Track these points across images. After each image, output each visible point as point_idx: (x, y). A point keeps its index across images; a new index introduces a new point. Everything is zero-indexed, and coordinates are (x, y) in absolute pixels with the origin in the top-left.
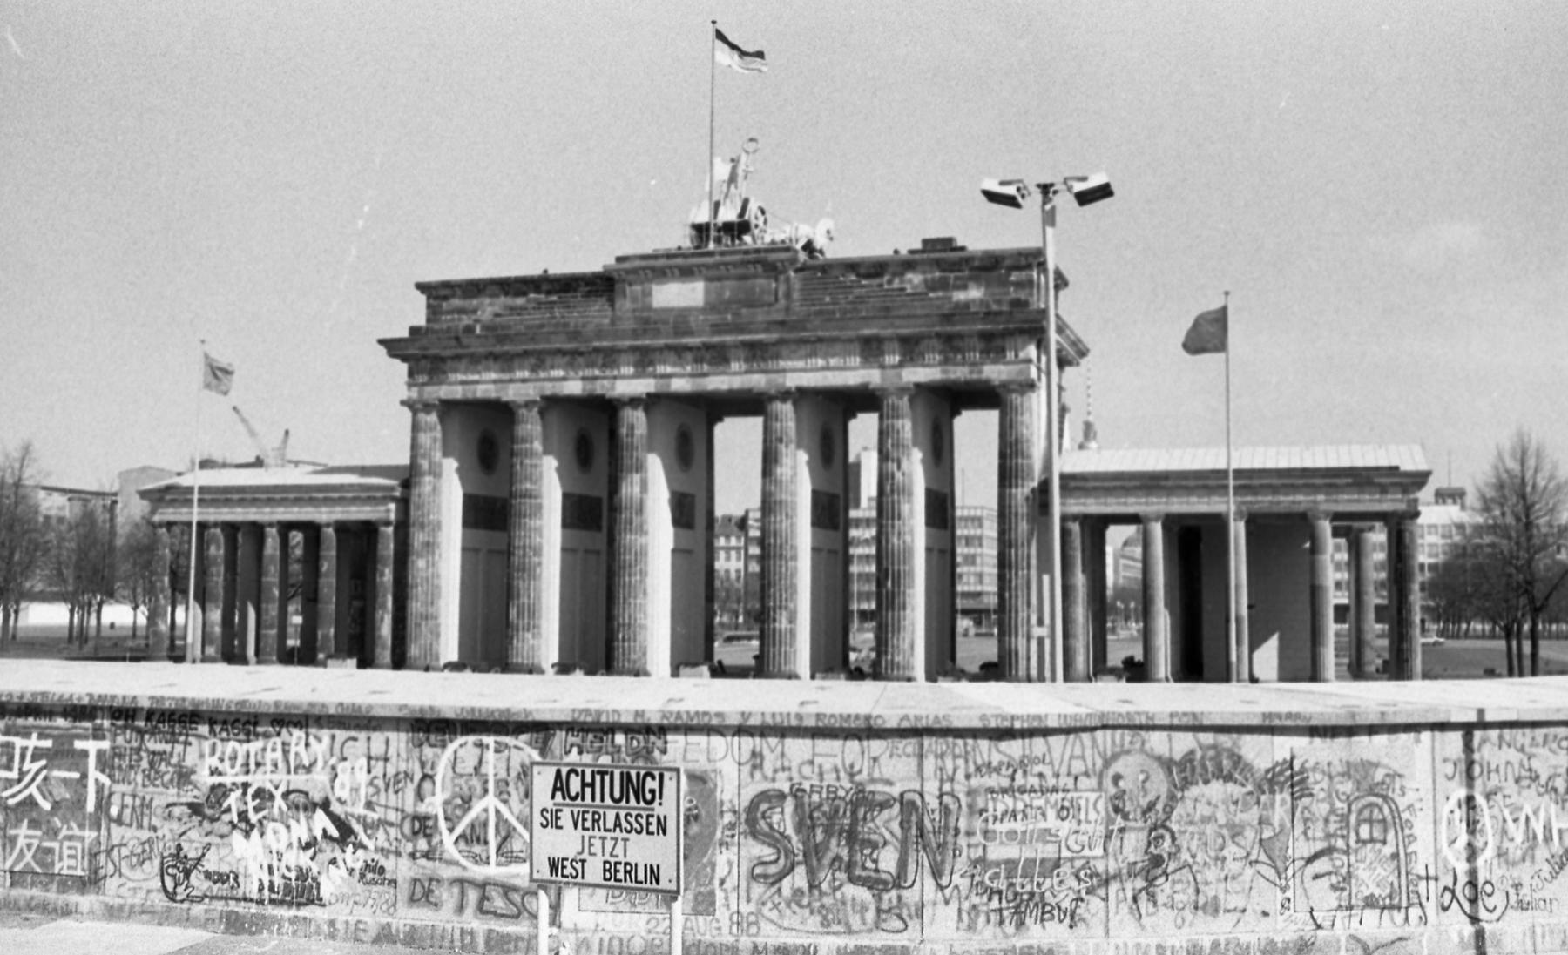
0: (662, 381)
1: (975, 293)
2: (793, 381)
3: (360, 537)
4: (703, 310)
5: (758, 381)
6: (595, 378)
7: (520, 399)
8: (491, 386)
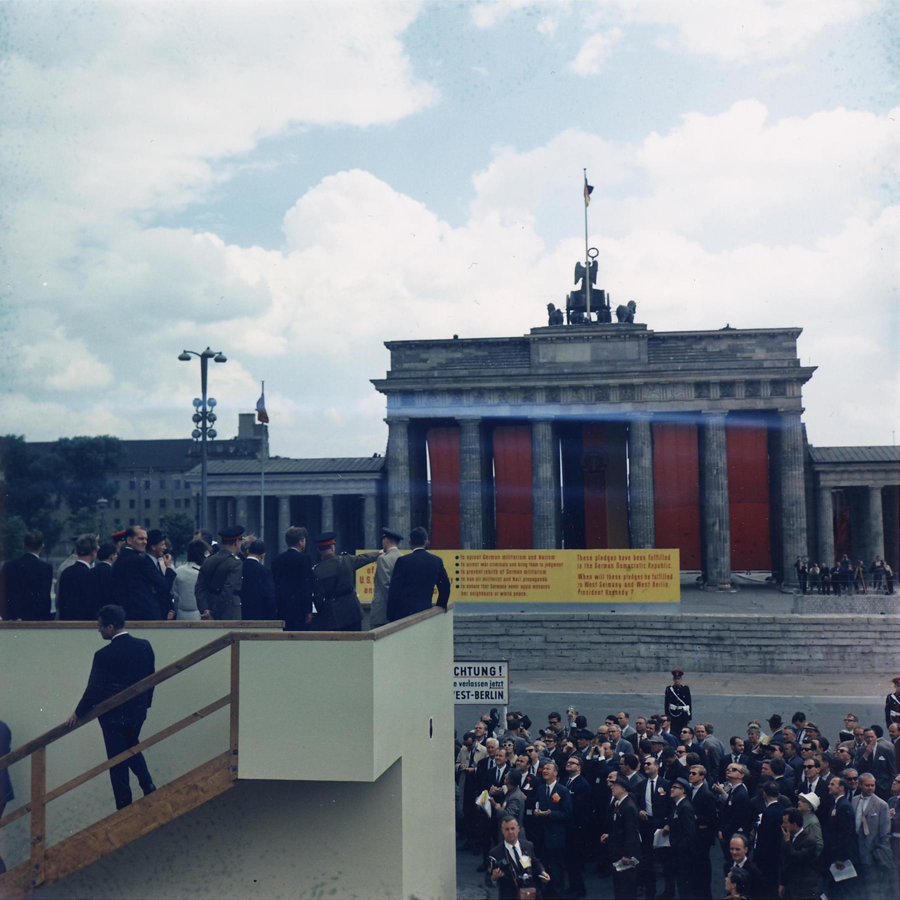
3: (349, 506)
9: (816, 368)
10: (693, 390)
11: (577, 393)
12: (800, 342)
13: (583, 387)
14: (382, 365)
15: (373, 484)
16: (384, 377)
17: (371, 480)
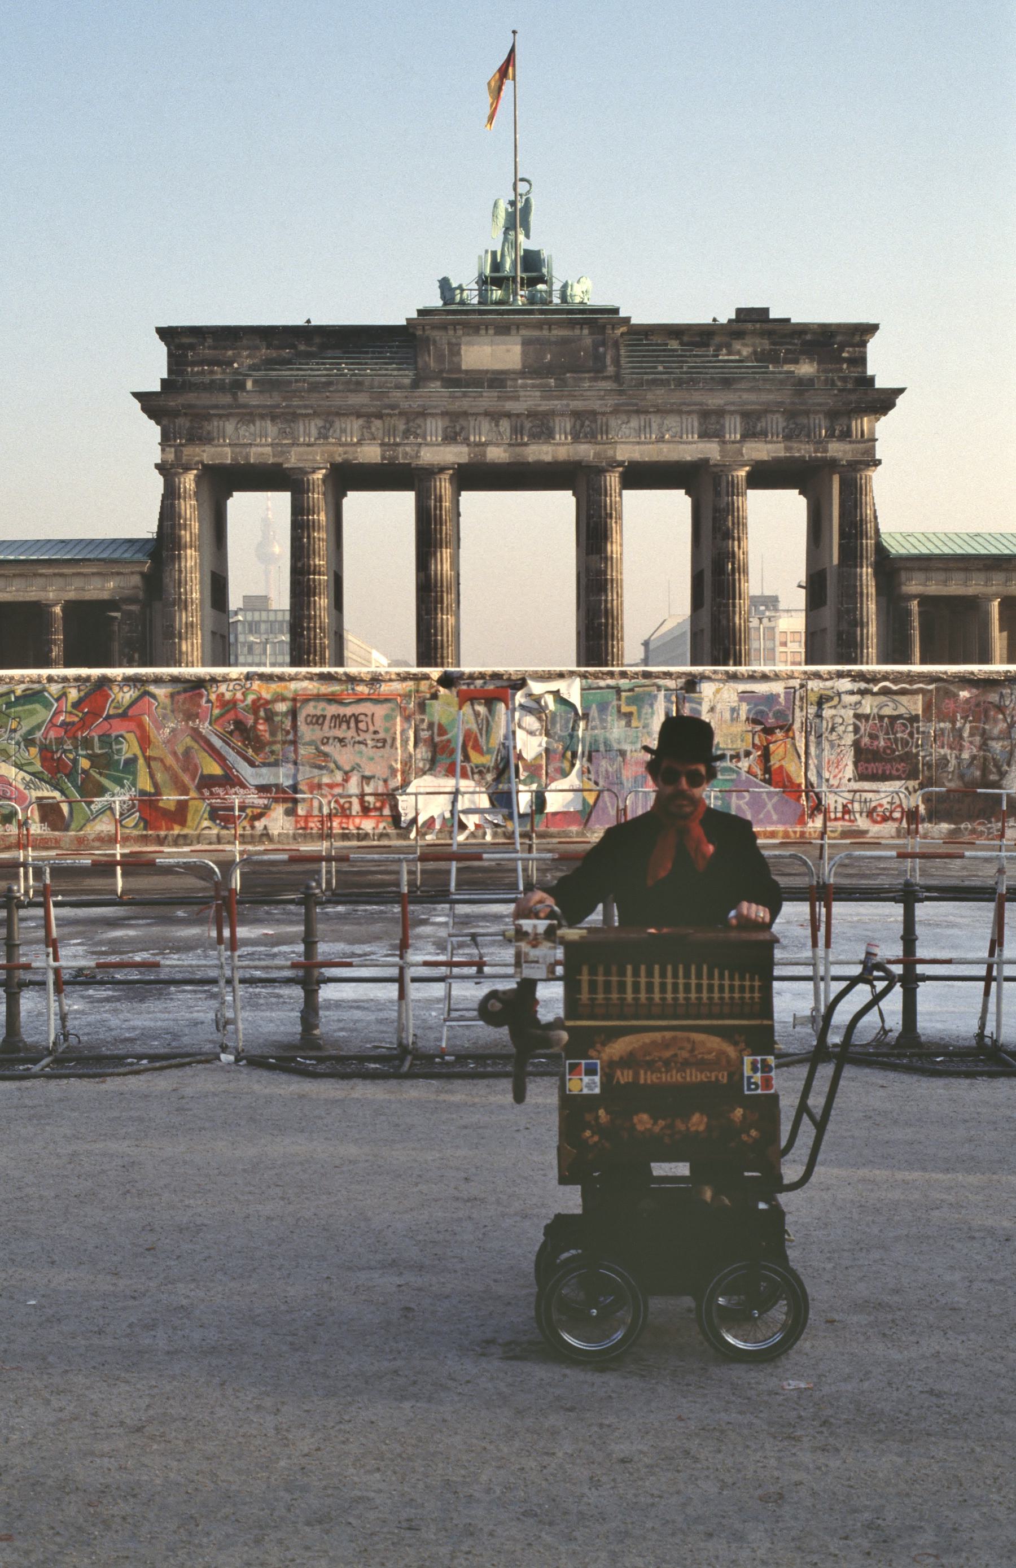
1: (806, 369)
2: (627, 452)
4: (522, 374)
5: (586, 451)
6: (398, 445)
8: (269, 449)
9: (901, 391)
10: (696, 424)
12: (874, 347)
13: (508, 415)
14: (153, 369)
15: (136, 580)
16: (157, 388)
17: (132, 573)
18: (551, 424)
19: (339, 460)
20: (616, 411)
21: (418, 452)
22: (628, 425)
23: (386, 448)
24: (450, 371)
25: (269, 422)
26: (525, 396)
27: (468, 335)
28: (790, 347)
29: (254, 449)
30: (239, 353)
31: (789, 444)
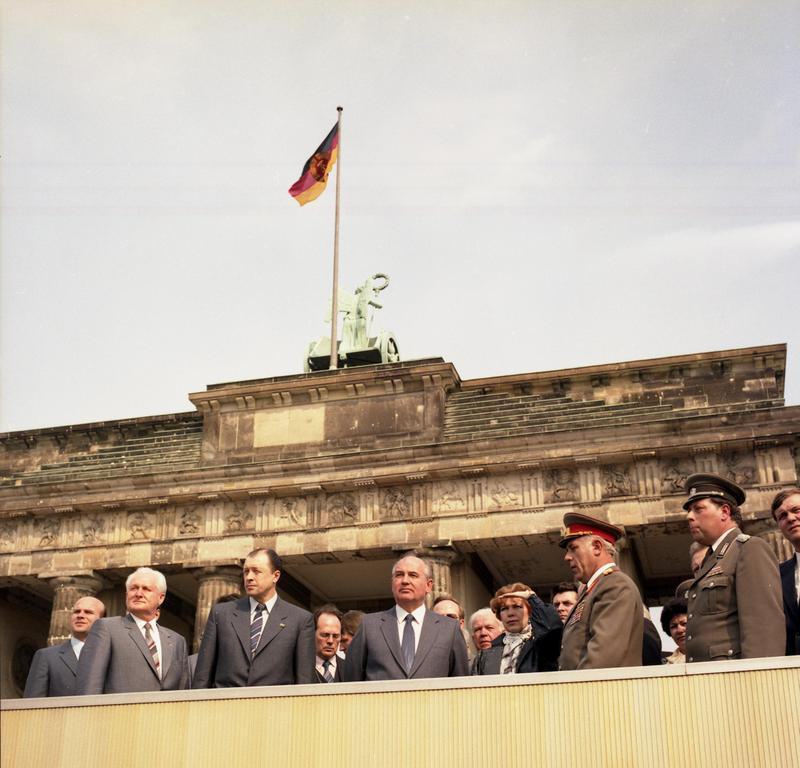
0: (264, 540)
7: (64, 575)
8: (28, 559)
11: (289, 506)
18: (356, 503)
19: (104, 565)
20: (433, 479)
21: (195, 549)
22: (456, 494)
23: (158, 547)
24: (239, 451)
25: (31, 527)
26: (316, 466)
27: (262, 408)
28: (670, 388)
29: (12, 559)
30: (30, 461)
31: (672, 500)
